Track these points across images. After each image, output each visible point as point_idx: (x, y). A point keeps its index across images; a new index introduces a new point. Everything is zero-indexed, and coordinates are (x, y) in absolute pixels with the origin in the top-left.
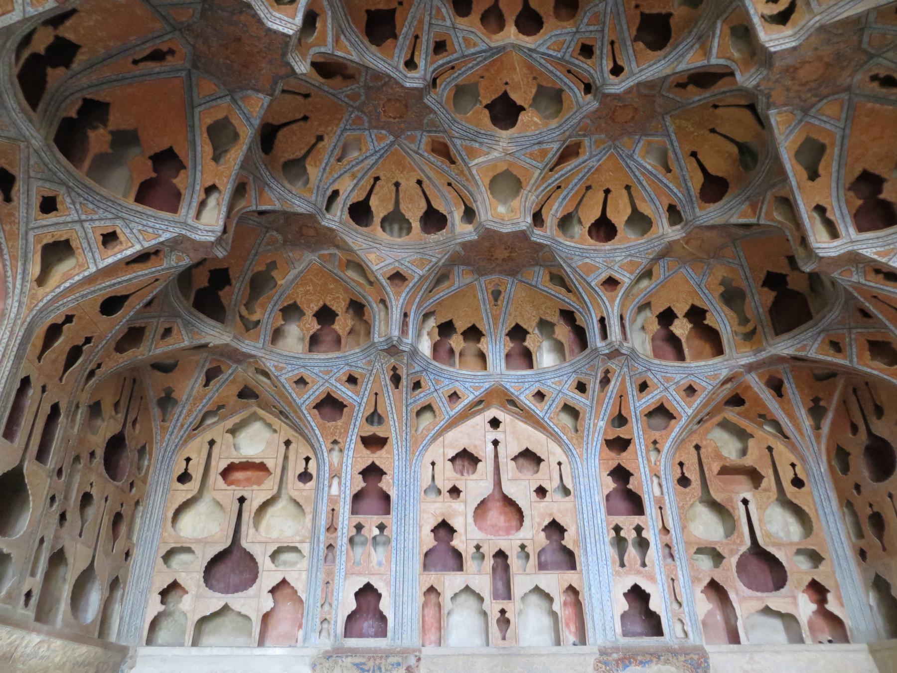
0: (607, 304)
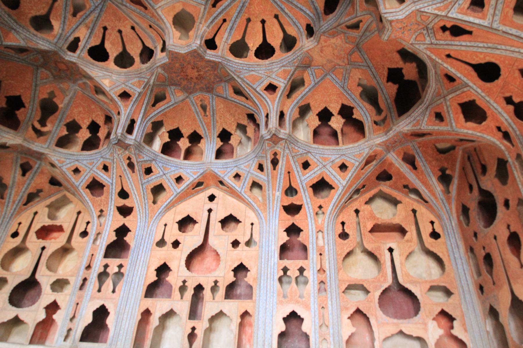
0: (270, 103)
